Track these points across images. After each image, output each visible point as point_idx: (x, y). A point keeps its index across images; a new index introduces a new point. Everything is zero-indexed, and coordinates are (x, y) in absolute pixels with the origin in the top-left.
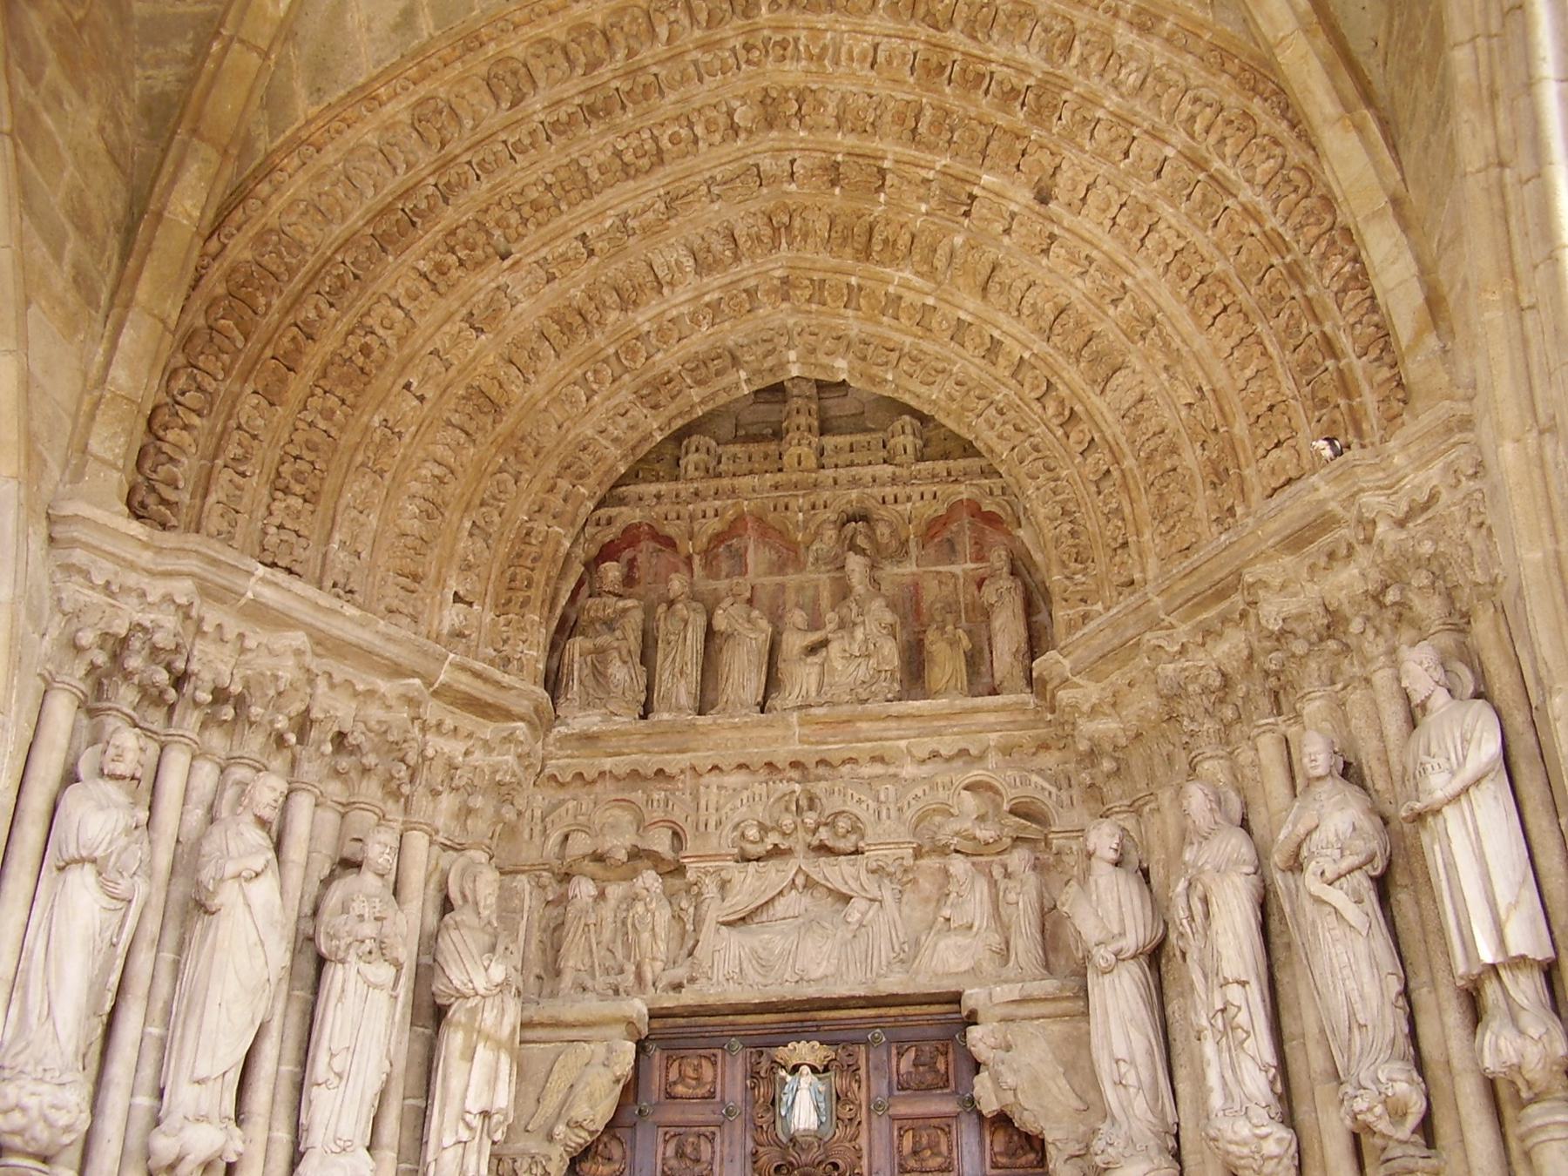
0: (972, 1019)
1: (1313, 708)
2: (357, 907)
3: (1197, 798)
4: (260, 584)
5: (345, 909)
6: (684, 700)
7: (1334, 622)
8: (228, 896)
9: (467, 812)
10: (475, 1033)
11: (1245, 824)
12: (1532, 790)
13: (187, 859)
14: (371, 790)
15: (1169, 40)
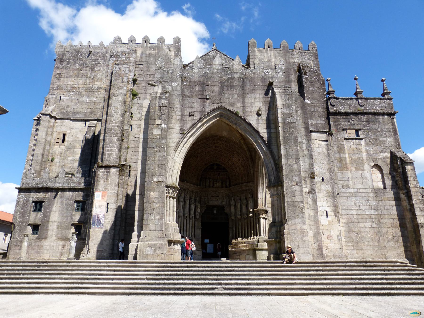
0: (225, 207)
1: (245, 194)
2: (192, 201)
3: (238, 198)
4: (188, 184)
5: (192, 201)
6: (208, 186)
7: (246, 190)
8: (187, 202)
9: (196, 194)
10: (198, 208)
11: (240, 200)
12: (254, 202)
13: (184, 199)
14: (191, 193)
15: (242, 149)
